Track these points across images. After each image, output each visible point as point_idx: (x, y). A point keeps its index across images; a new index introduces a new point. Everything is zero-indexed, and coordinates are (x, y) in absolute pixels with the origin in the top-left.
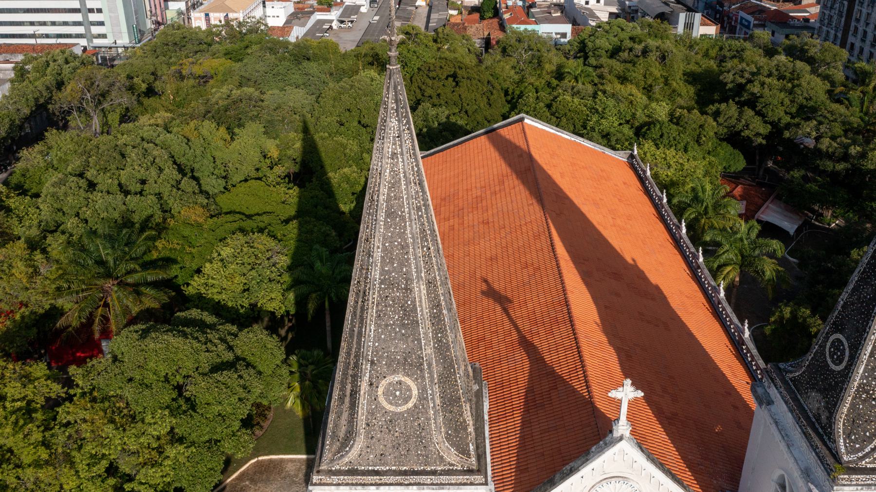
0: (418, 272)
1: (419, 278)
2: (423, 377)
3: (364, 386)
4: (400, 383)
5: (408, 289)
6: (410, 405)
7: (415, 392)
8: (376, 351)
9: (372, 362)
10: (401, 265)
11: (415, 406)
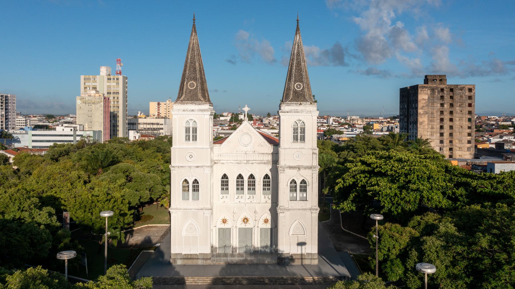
0: (197, 61)
1: (197, 62)
2: (197, 82)
3: (185, 83)
4: (192, 83)
5: (195, 64)
6: (194, 88)
7: (195, 85)
8: (188, 76)
9: (187, 79)
10: (194, 59)
11: (195, 88)
